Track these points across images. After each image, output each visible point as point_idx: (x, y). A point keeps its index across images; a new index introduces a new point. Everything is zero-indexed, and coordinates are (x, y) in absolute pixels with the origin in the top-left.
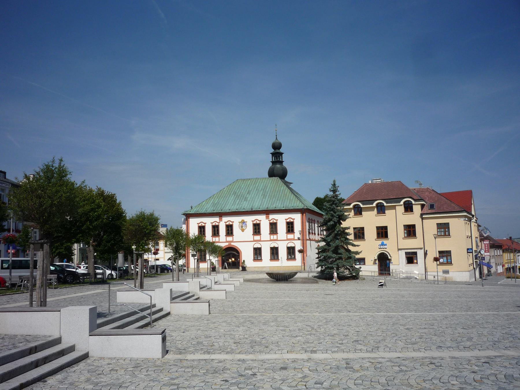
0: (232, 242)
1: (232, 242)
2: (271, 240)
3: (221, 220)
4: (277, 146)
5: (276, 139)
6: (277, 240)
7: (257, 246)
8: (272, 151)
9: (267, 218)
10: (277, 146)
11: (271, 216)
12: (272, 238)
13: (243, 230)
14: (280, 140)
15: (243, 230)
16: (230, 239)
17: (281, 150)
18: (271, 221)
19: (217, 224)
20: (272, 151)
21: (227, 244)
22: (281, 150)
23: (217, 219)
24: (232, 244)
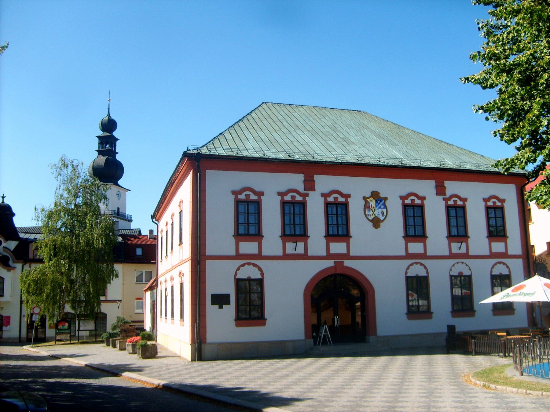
0: (347, 256)
1: (347, 256)
2: (452, 256)
3: (310, 185)
4: (109, 125)
5: (109, 116)
6: (467, 256)
7: (417, 271)
8: (100, 133)
9: (440, 190)
10: (109, 125)
11: (453, 187)
12: (455, 250)
13: (376, 223)
14: (113, 117)
15: (376, 223)
16: (338, 248)
17: (115, 134)
18: (451, 203)
19: (299, 198)
20: (100, 133)
21: (330, 263)
22: (115, 134)
23: (296, 181)
24: (347, 263)
